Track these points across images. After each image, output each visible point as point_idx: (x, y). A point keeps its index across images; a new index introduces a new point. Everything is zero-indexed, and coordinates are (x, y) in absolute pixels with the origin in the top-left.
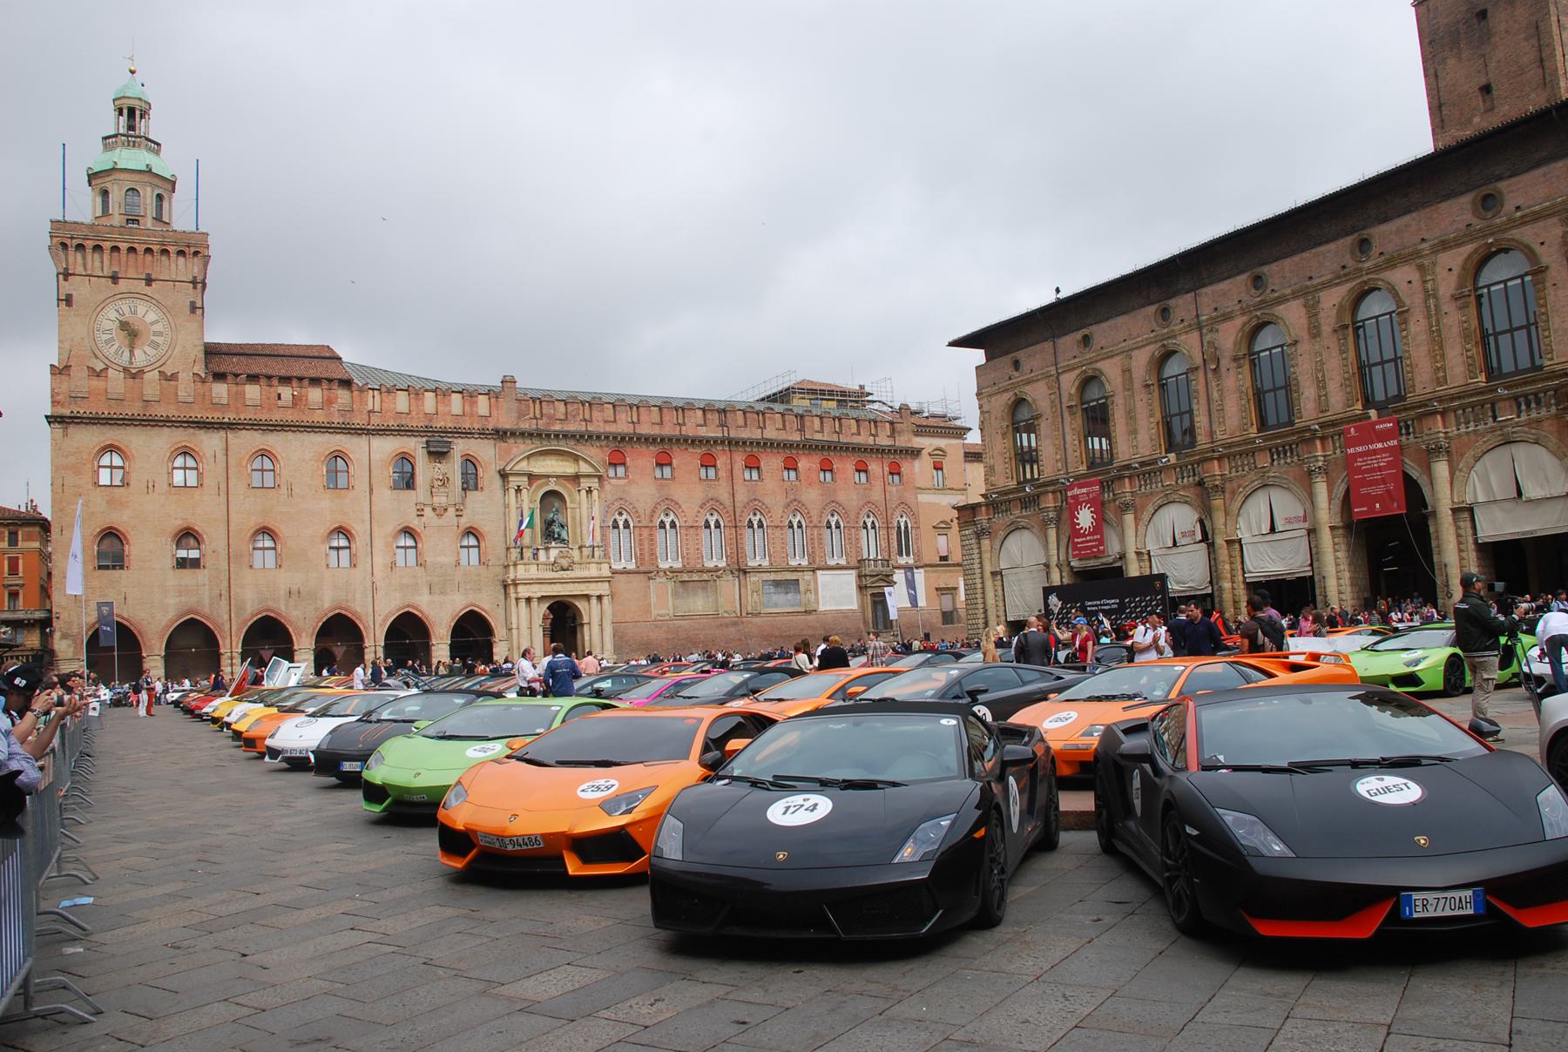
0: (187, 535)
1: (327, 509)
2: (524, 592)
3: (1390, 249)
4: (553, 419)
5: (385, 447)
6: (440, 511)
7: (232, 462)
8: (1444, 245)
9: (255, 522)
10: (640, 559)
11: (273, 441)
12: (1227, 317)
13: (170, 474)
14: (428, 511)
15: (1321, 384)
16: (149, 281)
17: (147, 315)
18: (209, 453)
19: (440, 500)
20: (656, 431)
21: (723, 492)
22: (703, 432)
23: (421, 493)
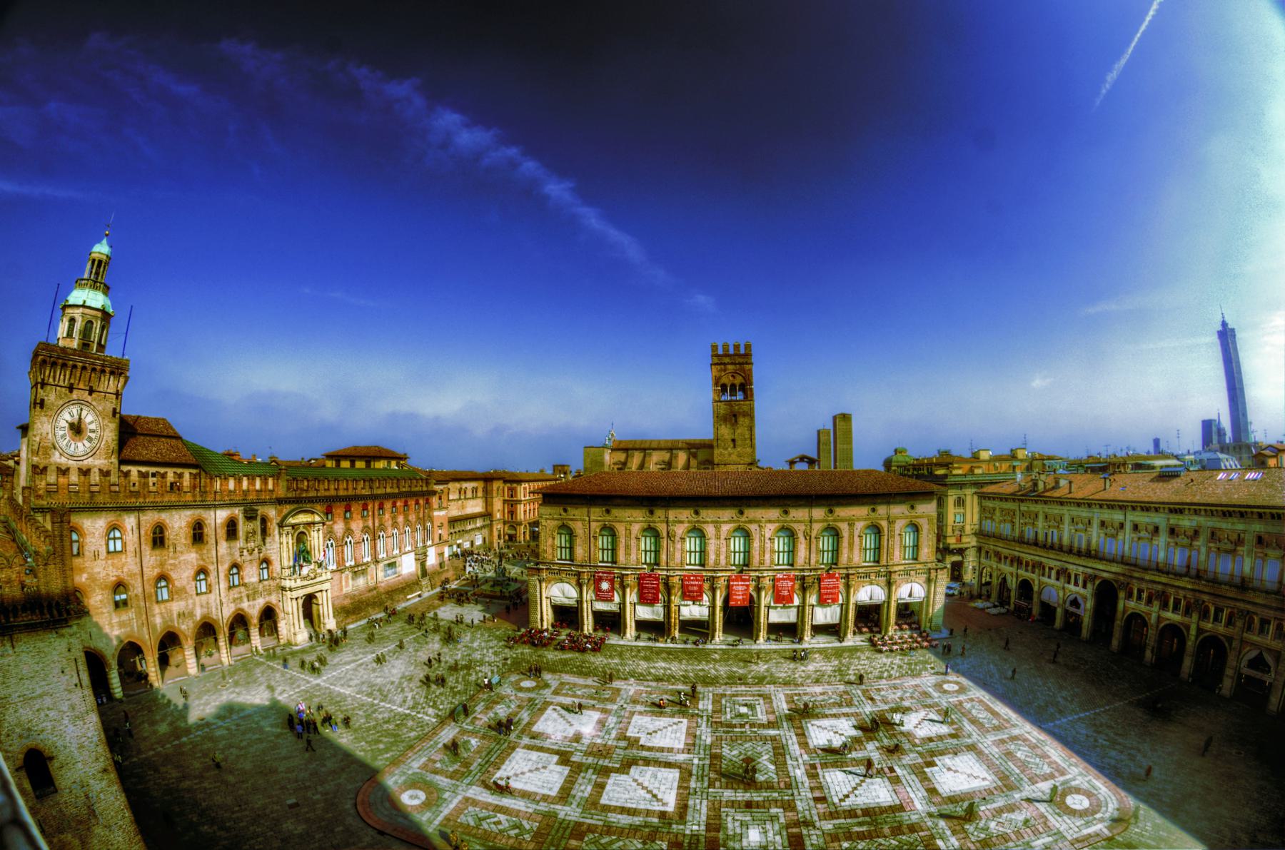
0: (119, 586)
1: (191, 557)
2: (295, 594)
3: (751, 517)
4: (302, 490)
5: (222, 515)
6: (251, 552)
7: (143, 532)
8: (770, 521)
9: (156, 571)
10: (338, 564)
11: (165, 517)
12: (682, 522)
13: (107, 545)
14: (245, 552)
15: (718, 555)
16: (91, 392)
17: (89, 417)
18: (129, 527)
19: (251, 545)
20: (346, 493)
21: (370, 523)
22: (364, 492)
23: (240, 543)
